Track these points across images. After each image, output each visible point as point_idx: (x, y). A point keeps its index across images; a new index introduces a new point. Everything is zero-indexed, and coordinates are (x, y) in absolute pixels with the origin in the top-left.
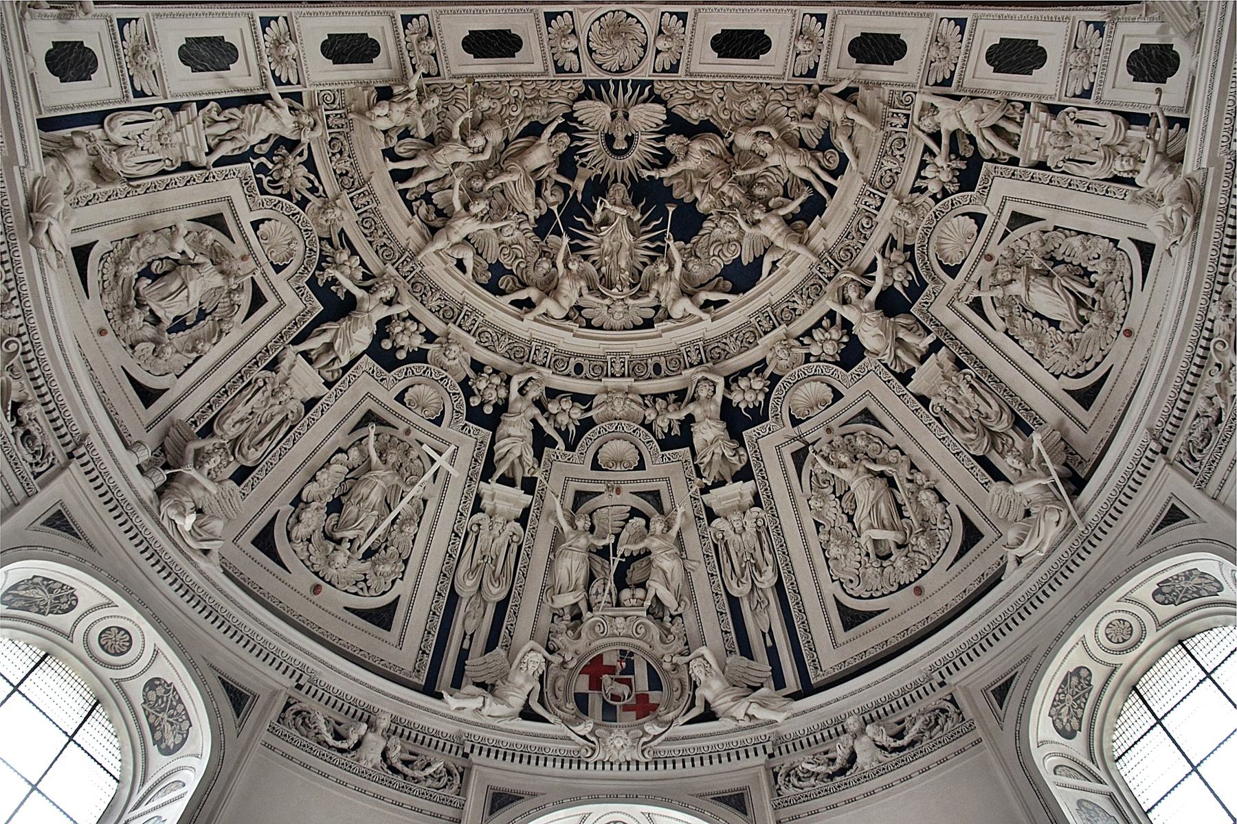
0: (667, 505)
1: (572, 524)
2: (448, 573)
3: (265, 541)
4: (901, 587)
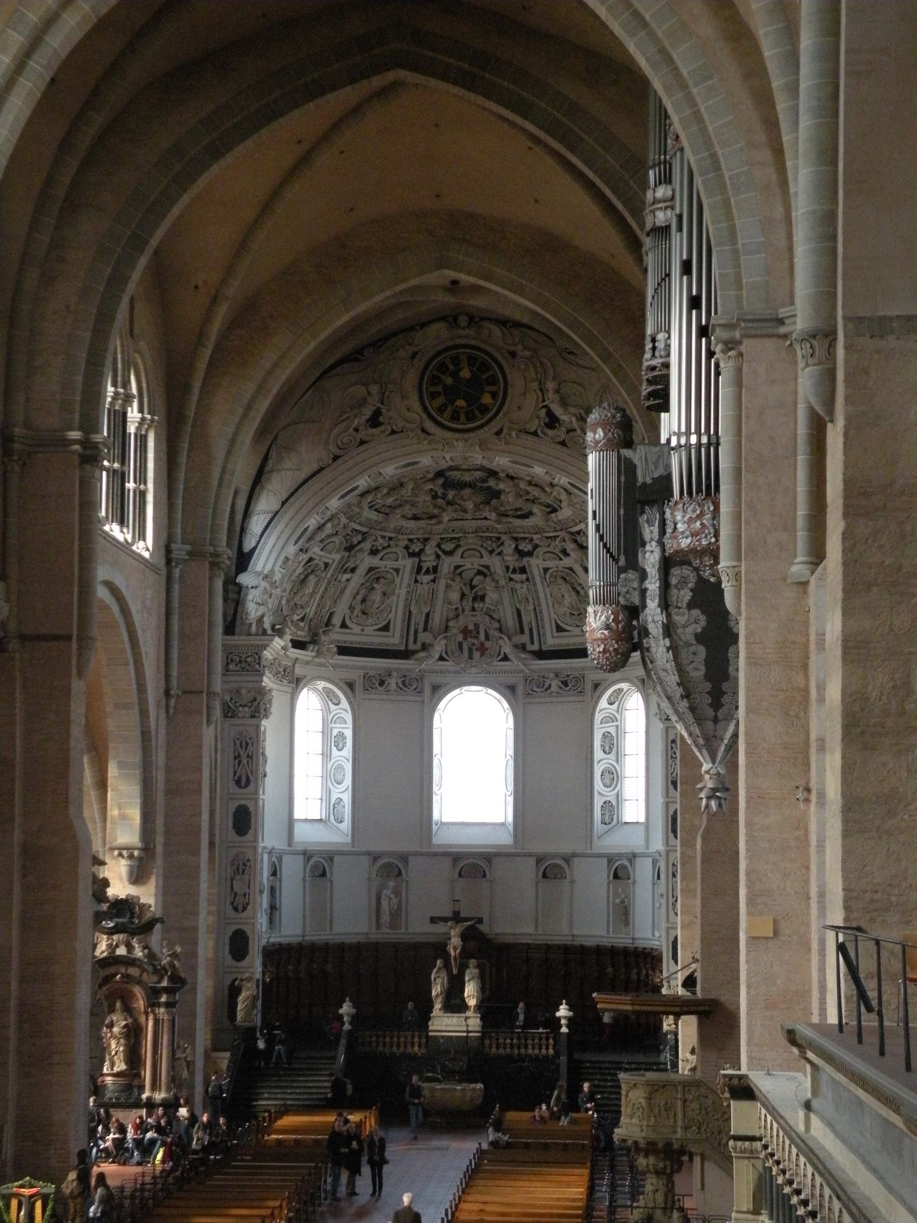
0: (492, 570)
1: (453, 580)
2: (407, 605)
3: (344, 625)
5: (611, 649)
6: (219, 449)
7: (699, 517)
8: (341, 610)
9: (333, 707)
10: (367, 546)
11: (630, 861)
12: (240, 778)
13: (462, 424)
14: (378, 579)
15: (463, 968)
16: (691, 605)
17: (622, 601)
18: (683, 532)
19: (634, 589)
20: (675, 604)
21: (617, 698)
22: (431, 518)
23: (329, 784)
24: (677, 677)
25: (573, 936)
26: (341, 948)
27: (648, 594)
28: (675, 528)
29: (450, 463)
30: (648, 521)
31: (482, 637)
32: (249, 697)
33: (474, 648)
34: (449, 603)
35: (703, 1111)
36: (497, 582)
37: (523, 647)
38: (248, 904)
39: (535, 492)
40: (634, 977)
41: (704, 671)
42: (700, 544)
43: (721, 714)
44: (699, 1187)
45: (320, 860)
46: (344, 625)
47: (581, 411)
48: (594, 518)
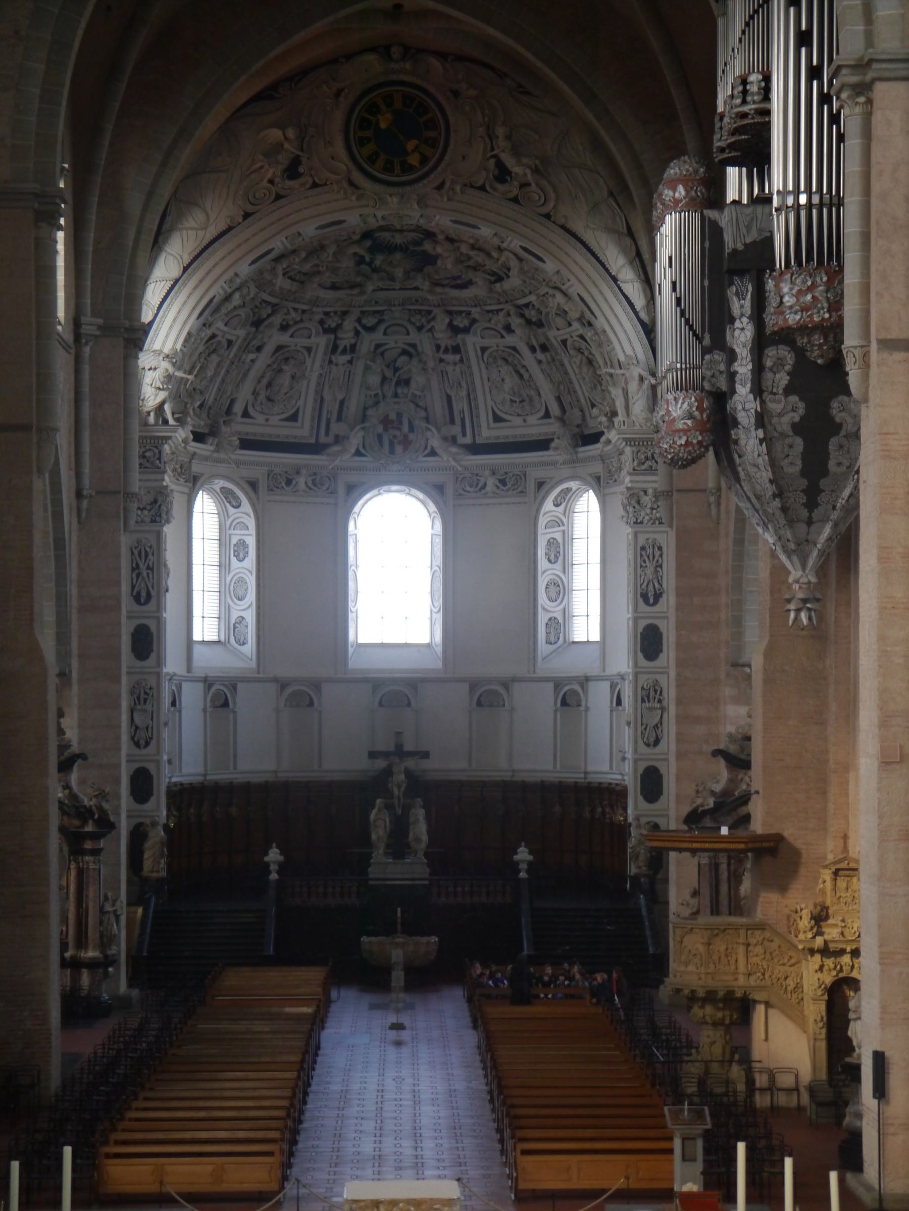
0: (420, 349)
1: (373, 361)
3: (246, 414)
4: (519, 415)
5: (695, 441)
6: (134, 203)
7: (810, 289)
8: (244, 395)
9: (232, 510)
10: (277, 320)
11: (582, 687)
12: (139, 593)
13: (397, 176)
14: (287, 359)
15: (407, 809)
16: (788, 391)
17: (707, 386)
18: (791, 307)
19: (721, 372)
20: (770, 389)
21: (566, 500)
22: (352, 286)
23: (229, 600)
24: (770, 475)
25: (514, 771)
26: (247, 788)
28: (781, 302)
29: (381, 223)
30: (737, 294)
31: (405, 428)
32: (150, 498)
33: (396, 441)
34: (368, 388)
35: (768, 956)
36: (425, 363)
37: (454, 440)
38: (151, 738)
39: (480, 258)
40: (587, 814)
41: (801, 466)
42: (812, 320)
43: (816, 515)
44: (763, 1036)
45: (222, 688)
46: (246, 414)
47: (537, 162)
48: (674, 289)
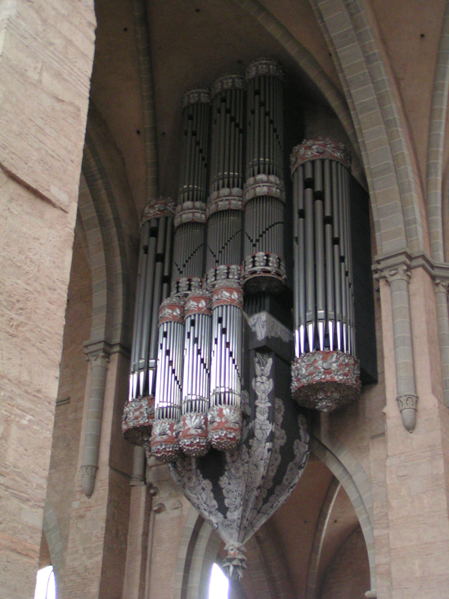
5: (237, 438)
7: (347, 365)
19: (247, 404)
24: (265, 472)
27: (258, 409)
30: (259, 362)
42: (348, 382)
